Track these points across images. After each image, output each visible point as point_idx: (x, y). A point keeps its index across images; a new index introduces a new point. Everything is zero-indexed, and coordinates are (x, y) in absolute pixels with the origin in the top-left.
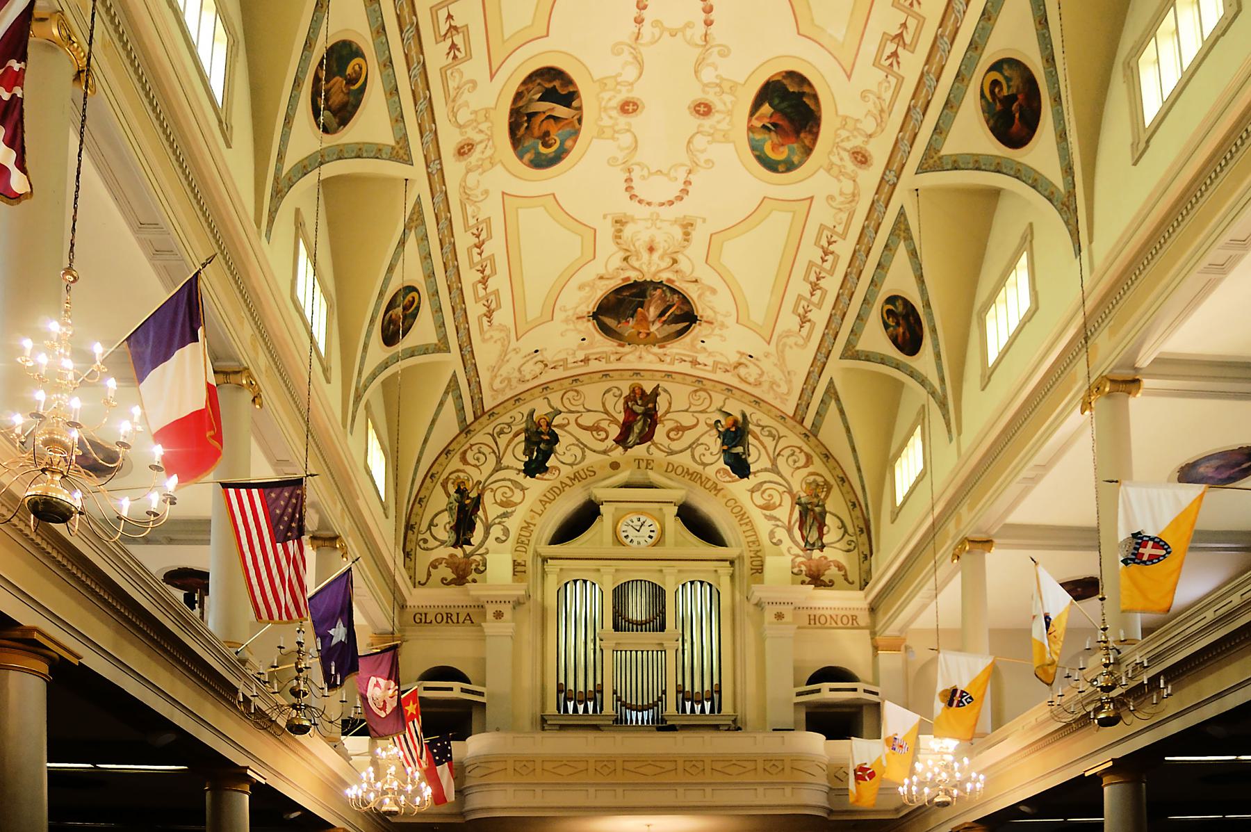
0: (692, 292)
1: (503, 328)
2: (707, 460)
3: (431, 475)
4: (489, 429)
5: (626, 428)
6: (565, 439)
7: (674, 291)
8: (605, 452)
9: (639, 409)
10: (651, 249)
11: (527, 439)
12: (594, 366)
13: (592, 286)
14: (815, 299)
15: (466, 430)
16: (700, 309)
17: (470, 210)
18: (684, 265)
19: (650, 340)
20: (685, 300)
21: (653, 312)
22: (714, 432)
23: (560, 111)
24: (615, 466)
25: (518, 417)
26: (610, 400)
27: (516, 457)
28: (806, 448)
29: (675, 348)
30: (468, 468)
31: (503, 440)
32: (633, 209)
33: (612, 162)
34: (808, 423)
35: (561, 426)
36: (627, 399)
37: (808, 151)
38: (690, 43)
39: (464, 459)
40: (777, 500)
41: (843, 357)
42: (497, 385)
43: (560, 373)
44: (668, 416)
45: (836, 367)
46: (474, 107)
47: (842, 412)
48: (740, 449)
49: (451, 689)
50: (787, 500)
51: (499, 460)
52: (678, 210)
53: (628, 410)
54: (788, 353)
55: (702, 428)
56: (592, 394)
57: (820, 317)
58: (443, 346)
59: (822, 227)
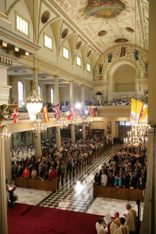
2: (132, 58)
3: (96, 64)
5: (121, 54)
8: (118, 58)
9: (123, 51)
11: (108, 57)
22: (133, 53)
25: (107, 54)
26: (119, 49)
27: (107, 60)
28: (147, 55)
30: (101, 62)
31: (105, 57)
35: (113, 54)
44: (127, 51)
50: (144, 63)
51: (105, 60)
53: (122, 51)
56: (117, 49)
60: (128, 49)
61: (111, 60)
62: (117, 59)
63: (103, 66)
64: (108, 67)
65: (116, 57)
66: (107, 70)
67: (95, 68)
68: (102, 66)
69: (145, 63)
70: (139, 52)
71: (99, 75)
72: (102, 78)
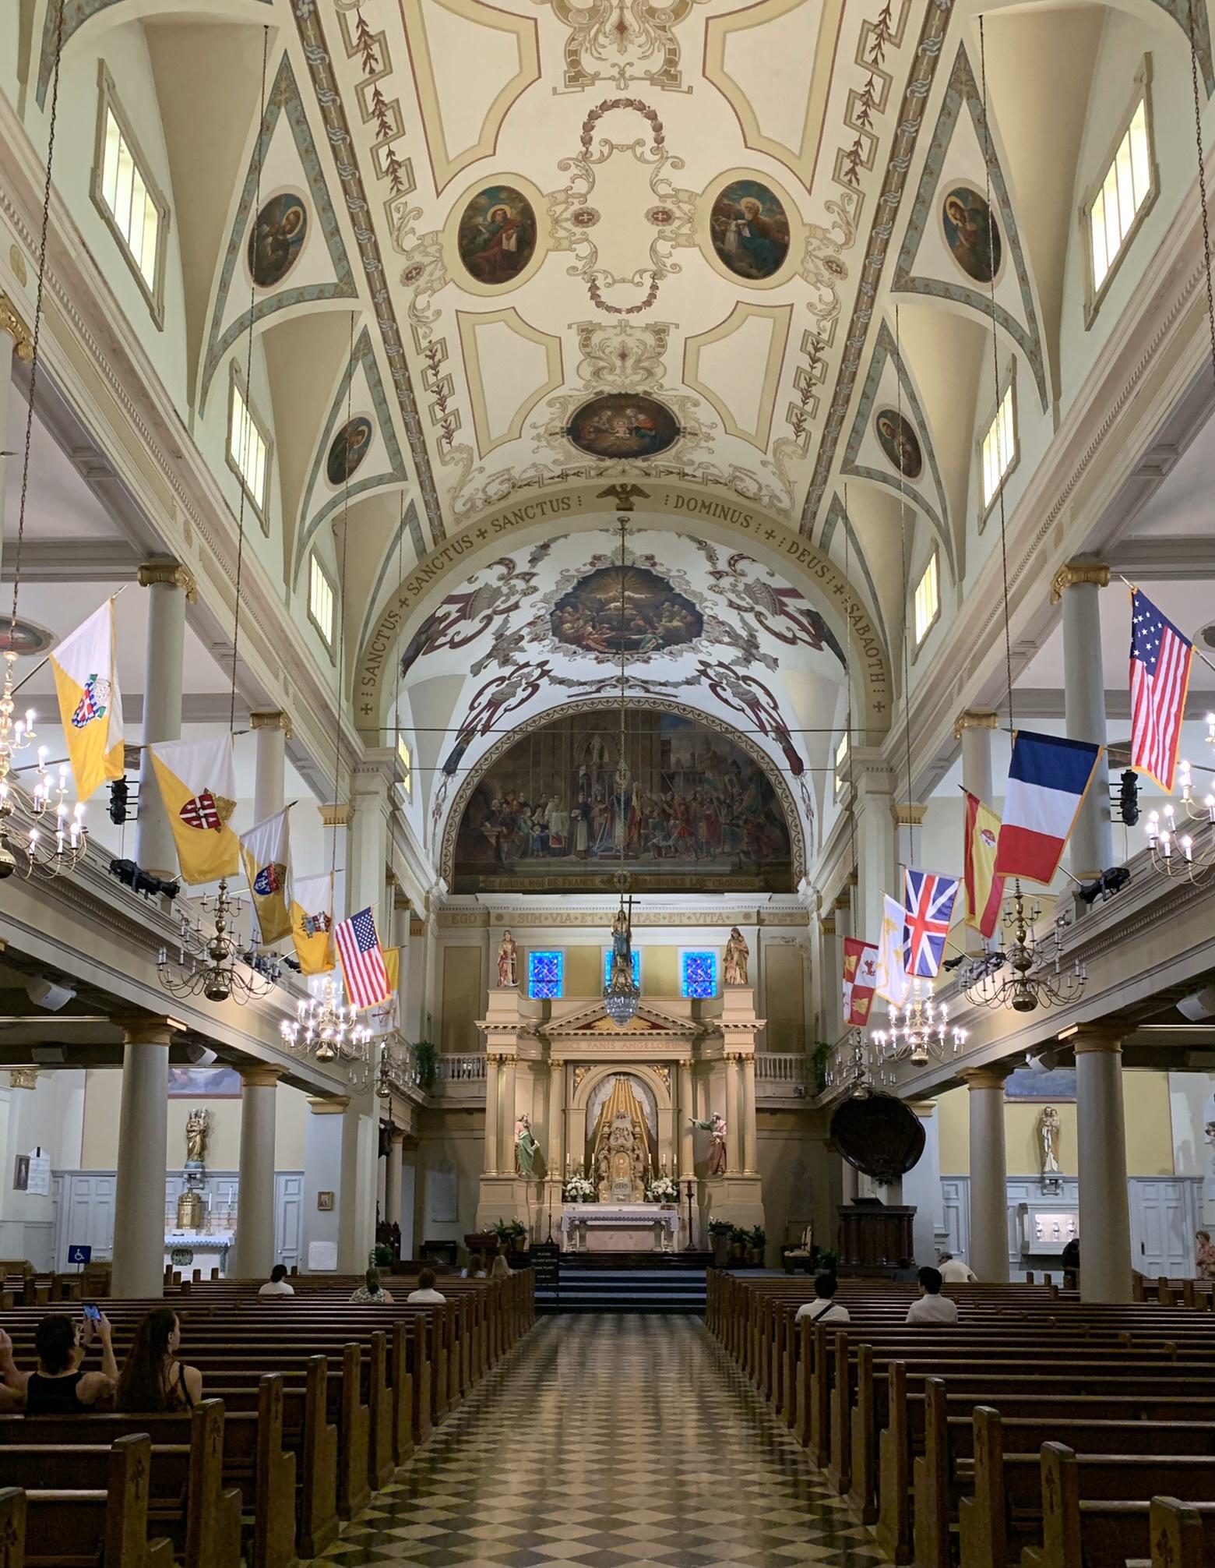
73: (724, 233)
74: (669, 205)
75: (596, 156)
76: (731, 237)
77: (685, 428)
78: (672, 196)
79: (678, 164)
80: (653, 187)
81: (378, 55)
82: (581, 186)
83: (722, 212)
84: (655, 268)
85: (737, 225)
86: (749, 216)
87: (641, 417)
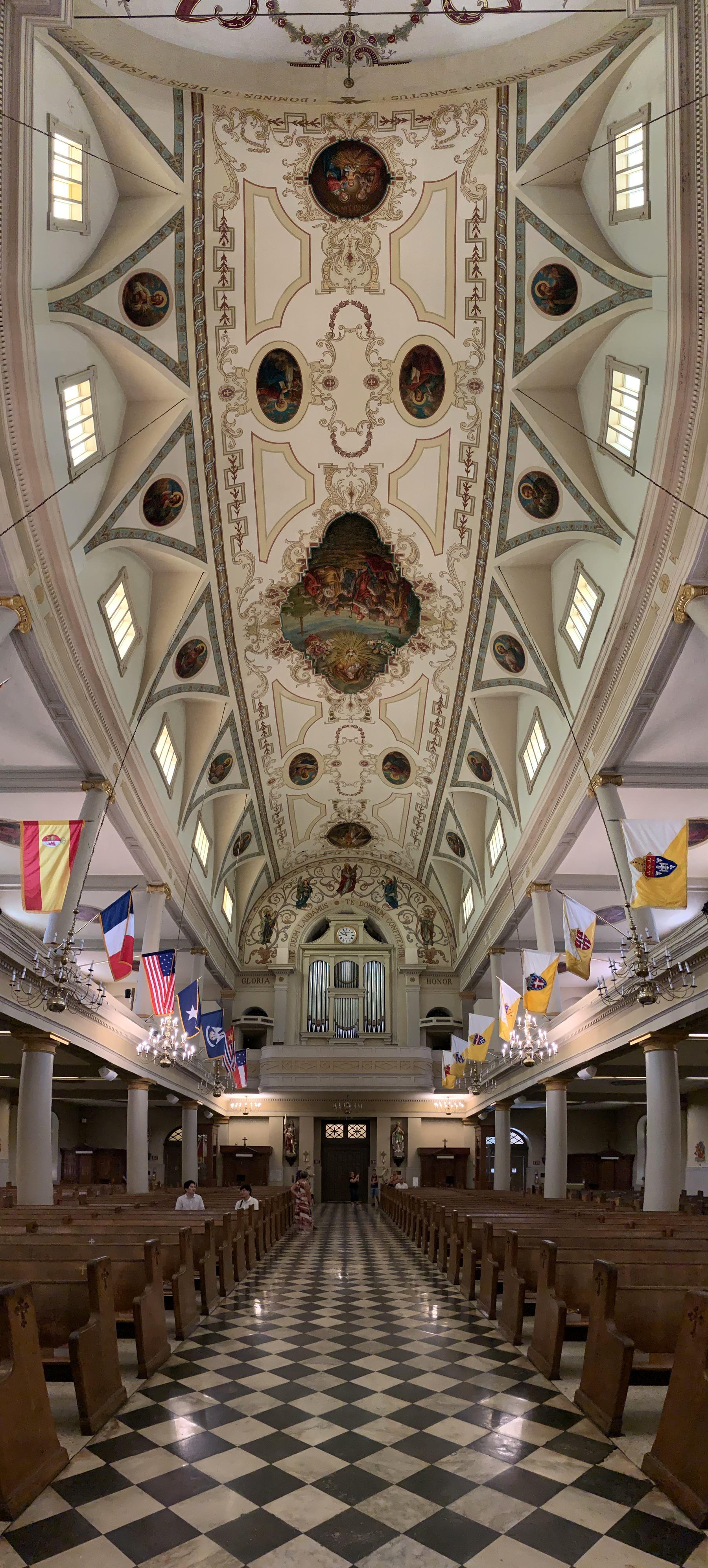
0: (369, 827)
1: (288, 844)
2: (379, 899)
3: (254, 908)
4: (282, 886)
6: (315, 890)
7: (361, 827)
8: (332, 896)
9: (348, 876)
10: (349, 811)
12: (329, 856)
13: (326, 825)
14: (419, 831)
15: (271, 886)
16: (372, 833)
17: (273, 802)
18: (363, 817)
19: (352, 846)
20: (366, 830)
21: (352, 835)
23: (309, 766)
24: (337, 903)
27: (293, 900)
29: (362, 849)
30: (271, 905)
32: (340, 797)
33: (331, 782)
34: (423, 882)
35: (314, 884)
36: (343, 872)
37: (407, 777)
38: (357, 743)
39: (270, 901)
40: (410, 919)
41: (434, 855)
42: (286, 866)
43: (314, 859)
45: (431, 859)
46: (275, 767)
47: (437, 879)
48: (393, 894)
49: (256, 1020)
50: (415, 918)
51: (285, 900)
52: (359, 797)
53: (344, 877)
54: (411, 852)
55: (376, 884)
56: (328, 869)
57: (422, 838)
58: (261, 853)
59: (417, 804)
60: (364, 871)
61: (306, 899)
62: (326, 899)
63: (279, 919)
64: (296, 922)
65: (323, 894)
66: (290, 932)
67: (248, 921)
68: (273, 918)
69: (420, 920)
70: (401, 885)
71: (260, 945)
72: (271, 959)
73: (294, 380)
74: (326, 392)
75: (365, 425)
76: (290, 377)
77: (306, 184)
78: (324, 399)
79: (323, 422)
80: (335, 405)
81: (459, 521)
82: (373, 405)
83: (296, 395)
84: (333, 342)
85: (287, 387)
86: (282, 397)
87: (337, 192)
